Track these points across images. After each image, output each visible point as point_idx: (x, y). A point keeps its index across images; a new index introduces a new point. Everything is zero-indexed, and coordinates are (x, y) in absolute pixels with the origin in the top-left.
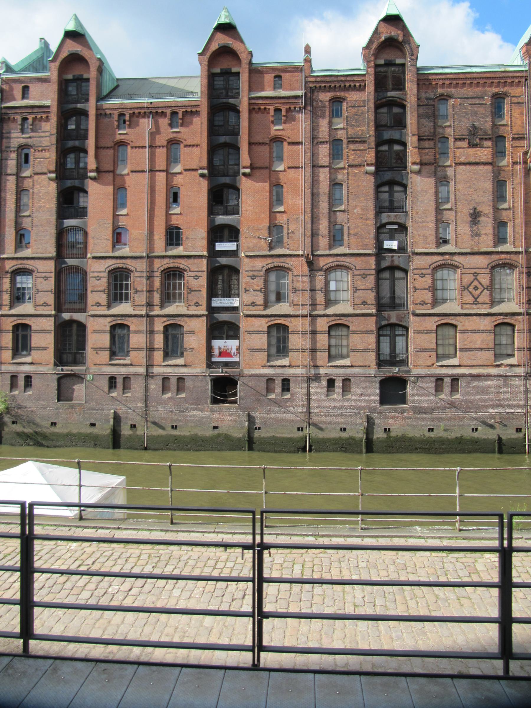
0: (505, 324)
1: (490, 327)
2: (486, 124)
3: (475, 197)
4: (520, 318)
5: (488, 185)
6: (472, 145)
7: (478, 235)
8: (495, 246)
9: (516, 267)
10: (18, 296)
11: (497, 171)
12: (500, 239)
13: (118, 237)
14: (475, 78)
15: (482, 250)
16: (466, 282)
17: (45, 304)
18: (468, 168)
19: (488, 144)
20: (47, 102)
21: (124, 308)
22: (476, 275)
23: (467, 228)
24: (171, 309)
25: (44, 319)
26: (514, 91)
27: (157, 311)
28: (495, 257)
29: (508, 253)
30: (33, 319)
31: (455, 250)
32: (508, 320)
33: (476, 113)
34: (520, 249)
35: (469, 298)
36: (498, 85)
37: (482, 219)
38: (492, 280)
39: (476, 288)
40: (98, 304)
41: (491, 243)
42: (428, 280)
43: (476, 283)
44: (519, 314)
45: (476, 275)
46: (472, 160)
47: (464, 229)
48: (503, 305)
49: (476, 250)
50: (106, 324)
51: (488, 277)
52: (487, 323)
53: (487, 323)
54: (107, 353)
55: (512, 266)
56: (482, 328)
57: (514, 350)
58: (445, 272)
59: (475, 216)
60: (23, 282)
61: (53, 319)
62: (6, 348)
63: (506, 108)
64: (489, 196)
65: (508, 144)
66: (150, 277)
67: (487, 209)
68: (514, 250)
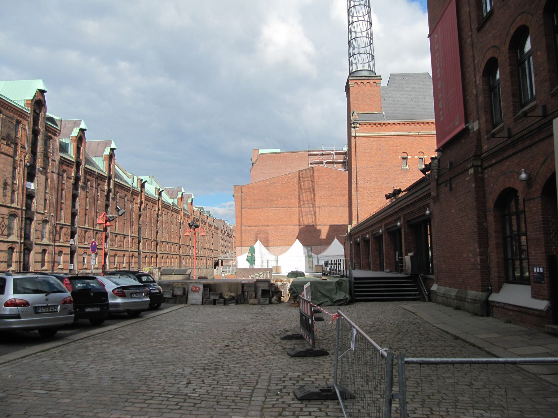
1: (6, 249)
3: (6, 174)
4: (17, 244)
5: (11, 169)
6: (8, 145)
8: (11, 204)
9: (17, 216)
11: (15, 162)
12: (12, 201)
14: (12, 108)
15: (7, 205)
18: (5, 157)
19: (13, 146)
22: (3, 218)
26: (24, 122)
29: (15, 208)
32: (13, 246)
33: (10, 127)
34: (20, 207)
37: (8, 187)
41: (10, 201)
43: (3, 223)
44: (17, 242)
45: (3, 218)
46: (6, 152)
48: (11, 237)
49: (4, 204)
56: (4, 249)
57: (12, 262)
59: (5, 184)
63: (20, 129)
64: (9, 176)
65: (19, 149)
67: (10, 182)
68: (17, 207)
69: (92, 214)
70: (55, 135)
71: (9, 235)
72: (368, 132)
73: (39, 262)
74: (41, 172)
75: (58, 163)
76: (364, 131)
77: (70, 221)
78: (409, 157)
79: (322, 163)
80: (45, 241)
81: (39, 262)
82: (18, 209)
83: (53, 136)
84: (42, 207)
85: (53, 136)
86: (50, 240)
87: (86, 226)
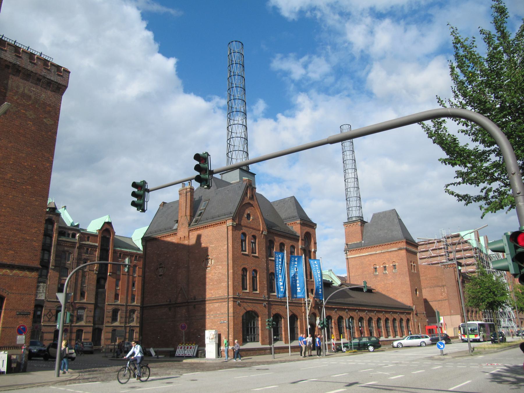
10: (80, 318)
13: (116, 297)
17: (90, 322)
21: (116, 324)
24: (131, 324)
25: (89, 328)
27: (128, 325)
30: (85, 328)
40: (108, 322)
50: (110, 329)
54: (110, 341)
60: (80, 312)
61: (92, 328)
62: (73, 340)
66: (126, 312)
72: (354, 255)
76: (351, 254)
78: (378, 267)
79: (427, 251)
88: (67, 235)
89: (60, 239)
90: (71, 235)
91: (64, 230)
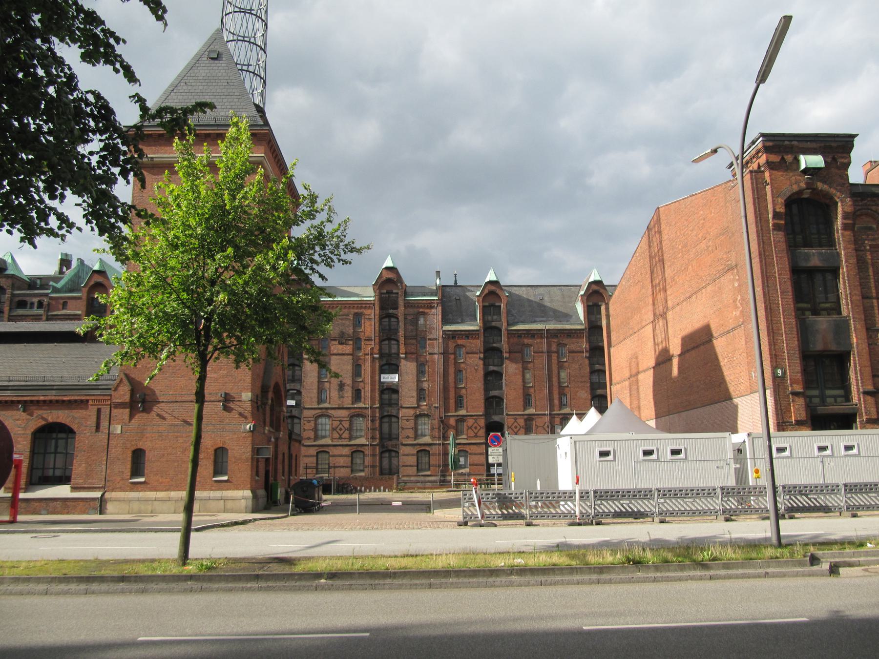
0: (357, 451)
1: (349, 453)
2: (350, 331)
6: (341, 343)
7: (343, 397)
8: (353, 404)
16: (334, 426)
18: (338, 357)
19: (351, 342)
20: (79, 312)
23: (337, 393)
28: (352, 411)
31: (329, 406)
32: (360, 449)
33: (343, 324)
35: (337, 436)
36: (357, 308)
37: (346, 388)
38: (351, 424)
39: (341, 429)
42: (312, 424)
44: (366, 445)
45: (341, 421)
46: (340, 352)
47: (334, 394)
51: (348, 423)
52: (346, 451)
53: (346, 451)
55: (363, 416)
58: (324, 419)
67: (348, 381)
69: (546, 391)
70: (432, 307)
71: (351, 438)
73: (411, 466)
74: (405, 358)
75: (441, 340)
77: (483, 409)
80: (427, 439)
81: (411, 466)
82: (366, 408)
83: (426, 311)
84: (414, 400)
85: (426, 311)
86: (433, 438)
87: (531, 411)
88: (29, 306)
89: (15, 314)
90: (36, 305)
91: (24, 299)
